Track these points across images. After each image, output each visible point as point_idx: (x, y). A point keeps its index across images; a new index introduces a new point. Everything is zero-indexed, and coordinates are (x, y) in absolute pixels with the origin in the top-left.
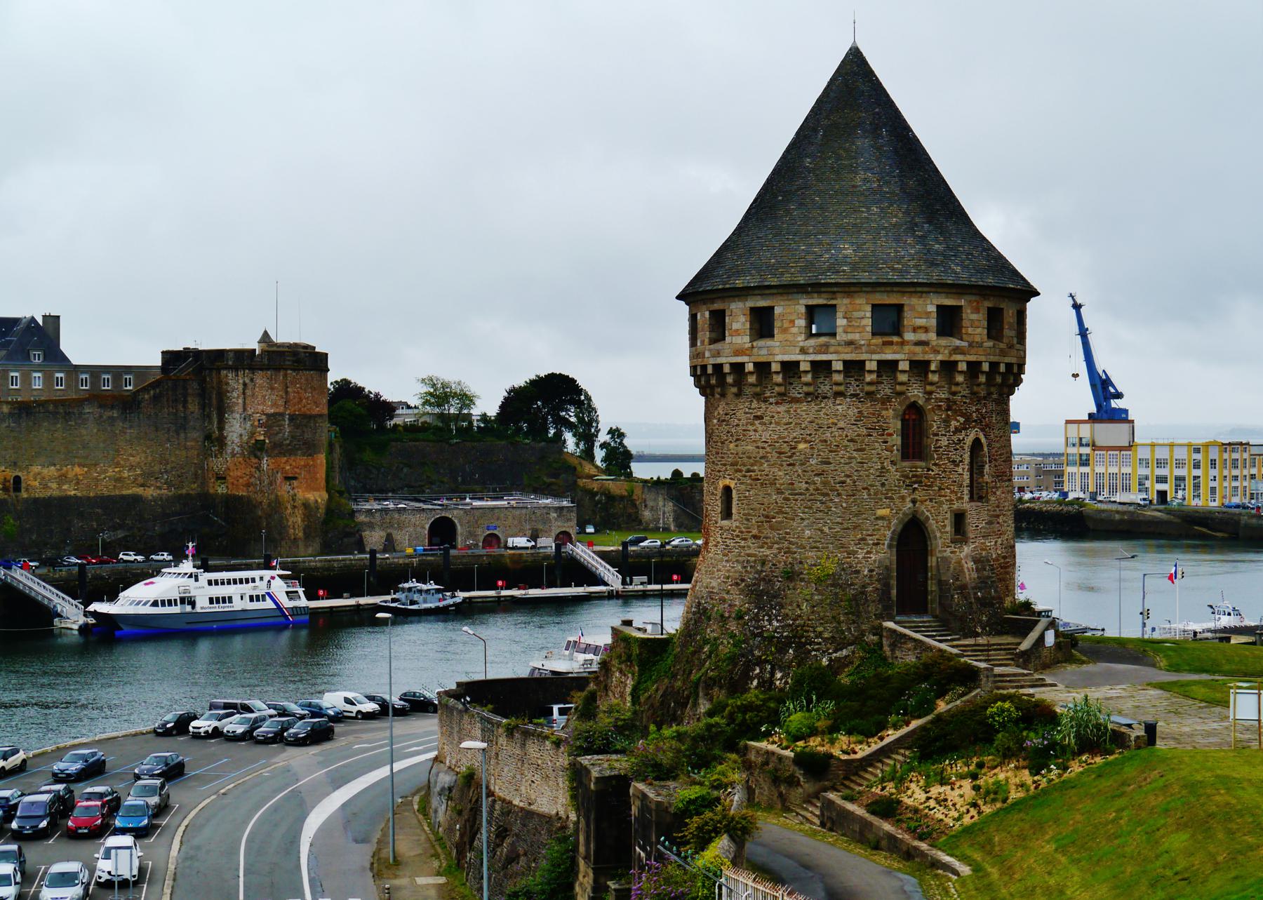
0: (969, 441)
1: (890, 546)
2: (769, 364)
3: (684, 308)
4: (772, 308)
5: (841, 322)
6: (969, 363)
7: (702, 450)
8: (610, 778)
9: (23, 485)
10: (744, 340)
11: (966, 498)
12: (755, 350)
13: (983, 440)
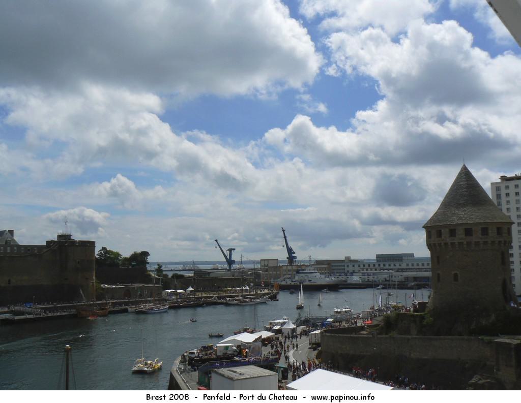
5: (490, 231)
10: (463, 236)
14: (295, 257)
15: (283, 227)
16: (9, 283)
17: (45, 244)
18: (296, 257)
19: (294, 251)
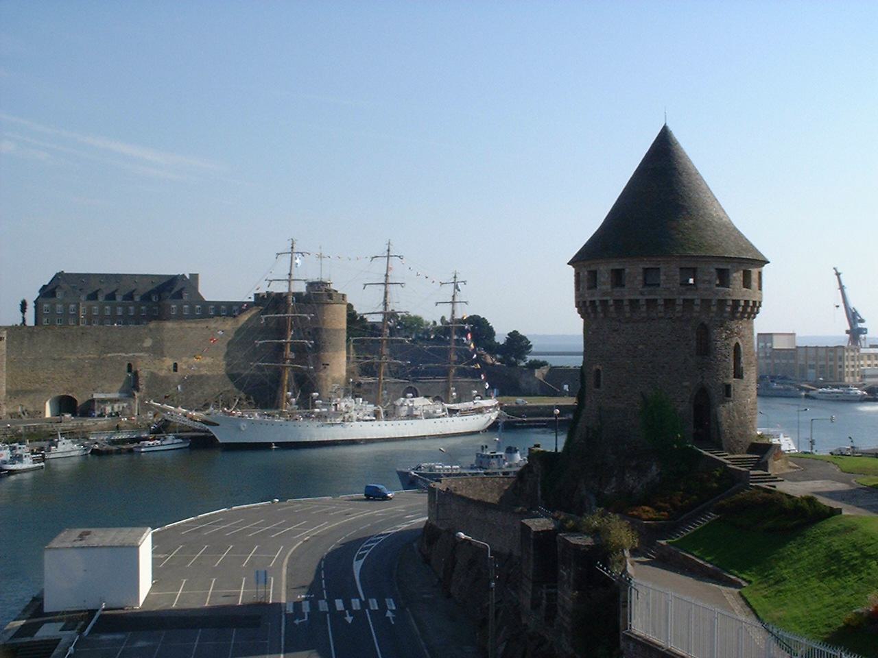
0: (733, 345)
1: (690, 402)
2: (622, 301)
3: (572, 270)
4: (624, 269)
5: (663, 277)
6: (733, 300)
7: (582, 349)
8: (542, 531)
9: (179, 368)
11: (732, 376)
12: (614, 293)
13: (740, 344)
14: (863, 331)
15: (835, 266)
16: (175, 370)
17: (252, 300)
18: (866, 329)
19: (863, 317)
